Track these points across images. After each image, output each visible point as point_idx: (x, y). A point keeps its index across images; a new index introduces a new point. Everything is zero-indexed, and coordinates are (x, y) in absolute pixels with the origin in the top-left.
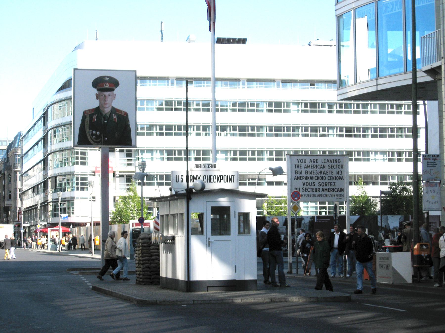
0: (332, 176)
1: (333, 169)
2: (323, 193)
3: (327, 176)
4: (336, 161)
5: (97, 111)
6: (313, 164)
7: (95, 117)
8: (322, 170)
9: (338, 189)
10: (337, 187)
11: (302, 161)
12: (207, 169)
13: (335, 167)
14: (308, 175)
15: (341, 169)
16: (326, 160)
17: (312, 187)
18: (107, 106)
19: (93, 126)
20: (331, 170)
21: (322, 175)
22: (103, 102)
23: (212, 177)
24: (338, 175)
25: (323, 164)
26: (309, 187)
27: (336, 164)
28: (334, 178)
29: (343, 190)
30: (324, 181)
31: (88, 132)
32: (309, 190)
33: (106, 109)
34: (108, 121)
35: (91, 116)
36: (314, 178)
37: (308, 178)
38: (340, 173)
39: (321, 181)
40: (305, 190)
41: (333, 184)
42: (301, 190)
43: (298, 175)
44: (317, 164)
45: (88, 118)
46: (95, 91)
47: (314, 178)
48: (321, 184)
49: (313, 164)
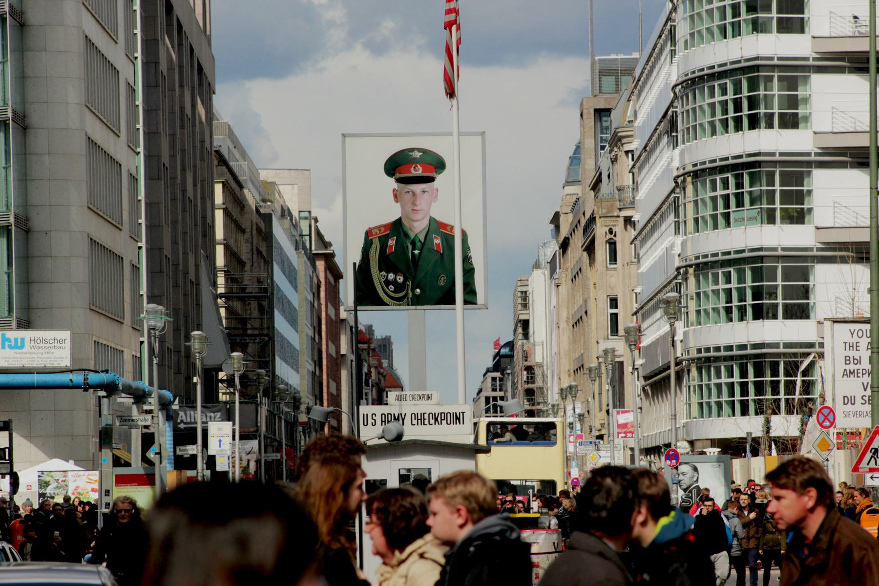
5: (397, 227)
7: (392, 242)
11: (860, 334)
12: (416, 402)
18: (419, 216)
19: (386, 264)
22: (409, 207)
23: (426, 416)
31: (377, 276)
33: (416, 224)
34: (421, 250)
35: (384, 241)
42: (859, 401)
43: (852, 367)
45: (376, 244)
46: (391, 183)
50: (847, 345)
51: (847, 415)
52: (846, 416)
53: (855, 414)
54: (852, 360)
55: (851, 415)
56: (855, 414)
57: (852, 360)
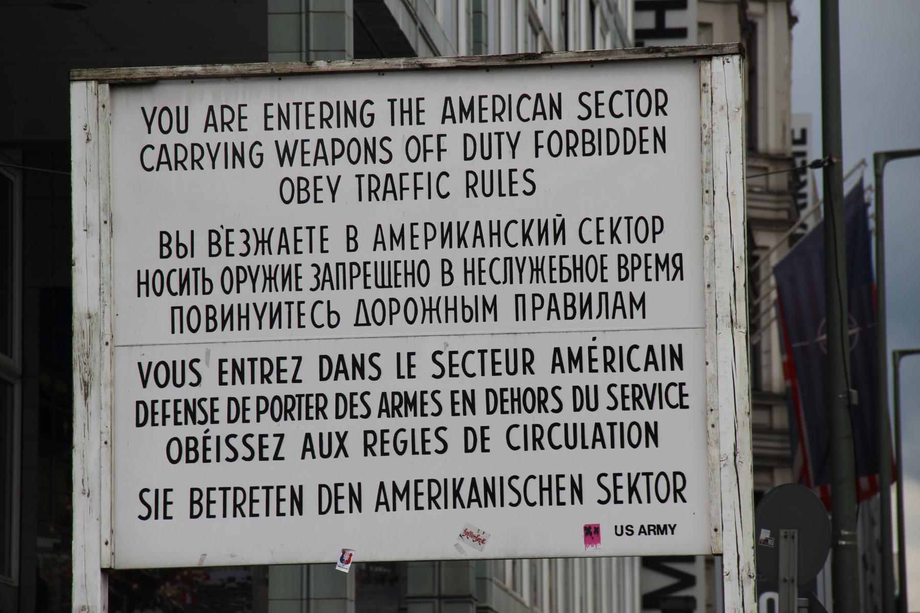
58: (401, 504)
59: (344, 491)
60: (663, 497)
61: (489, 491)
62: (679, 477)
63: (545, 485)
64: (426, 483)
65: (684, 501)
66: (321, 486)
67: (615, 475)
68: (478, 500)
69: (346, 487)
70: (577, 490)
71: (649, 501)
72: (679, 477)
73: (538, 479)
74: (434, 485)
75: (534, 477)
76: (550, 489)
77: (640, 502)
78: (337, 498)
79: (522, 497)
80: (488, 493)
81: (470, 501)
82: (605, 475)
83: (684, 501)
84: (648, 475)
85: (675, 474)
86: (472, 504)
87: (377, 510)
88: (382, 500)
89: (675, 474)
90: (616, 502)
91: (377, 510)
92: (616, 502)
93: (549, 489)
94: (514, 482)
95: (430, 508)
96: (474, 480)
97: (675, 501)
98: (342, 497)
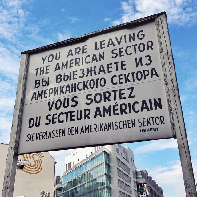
0: (123, 73)
1: (125, 57)
2: (100, 120)
3: (108, 76)
4: (132, 38)
6: (74, 57)
8: (97, 65)
9: (144, 102)
10: (139, 99)
11: (51, 58)
13: (131, 50)
14: (63, 83)
15: (146, 52)
16: (106, 43)
17: (70, 109)
20: (119, 59)
21: (94, 77)
24: (140, 68)
25: (97, 53)
26: (63, 110)
27: (133, 43)
28: (130, 78)
29: (158, 104)
30: (101, 90)
32: (63, 118)
36: (75, 87)
37: (62, 91)
38: (145, 61)
39: (94, 91)
40: (52, 119)
41: (128, 92)
42: (44, 120)
43: (41, 89)
44: (85, 55)
47: (75, 87)
48: (92, 97)
49: (74, 57)
50: (39, 70)
51: (30, 138)
52: (30, 139)
53: (38, 136)
54: (41, 83)
55: (35, 138)
56: (38, 136)
57: (41, 83)
58: (87, 131)
59: (74, 129)
60: (158, 124)
61: (110, 126)
62: (162, 118)
63: (125, 123)
64: (93, 125)
65: (164, 124)
66: (68, 128)
67: (143, 119)
68: (107, 128)
69: (74, 128)
70: (133, 124)
71: (153, 125)
72: (162, 118)
73: (123, 122)
74: (95, 126)
75: (121, 121)
76: (126, 124)
77: (151, 125)
78: (72, 131)
79: (118, 127)
80: (109, 127)
81: (105, 129)
82: (141, 119)
83: (164, 124)
84: (153, 118)
85: (161, 117)
86: (105, 129)
87: (81, 133)
88: (82, 130)
89: (161, 117)
90: (144, 126)
91: (81, 133)
92: (144, 126)
93: (126, 124)
94: (116, 123)
95: (94, 132)
96: (105, 123)
97: (161, 124)
98: (73, 131)
